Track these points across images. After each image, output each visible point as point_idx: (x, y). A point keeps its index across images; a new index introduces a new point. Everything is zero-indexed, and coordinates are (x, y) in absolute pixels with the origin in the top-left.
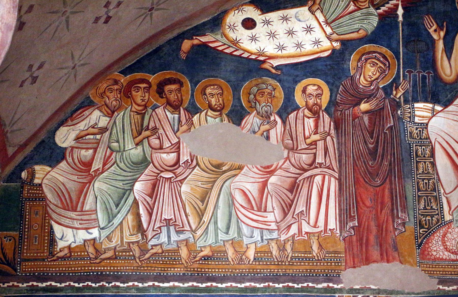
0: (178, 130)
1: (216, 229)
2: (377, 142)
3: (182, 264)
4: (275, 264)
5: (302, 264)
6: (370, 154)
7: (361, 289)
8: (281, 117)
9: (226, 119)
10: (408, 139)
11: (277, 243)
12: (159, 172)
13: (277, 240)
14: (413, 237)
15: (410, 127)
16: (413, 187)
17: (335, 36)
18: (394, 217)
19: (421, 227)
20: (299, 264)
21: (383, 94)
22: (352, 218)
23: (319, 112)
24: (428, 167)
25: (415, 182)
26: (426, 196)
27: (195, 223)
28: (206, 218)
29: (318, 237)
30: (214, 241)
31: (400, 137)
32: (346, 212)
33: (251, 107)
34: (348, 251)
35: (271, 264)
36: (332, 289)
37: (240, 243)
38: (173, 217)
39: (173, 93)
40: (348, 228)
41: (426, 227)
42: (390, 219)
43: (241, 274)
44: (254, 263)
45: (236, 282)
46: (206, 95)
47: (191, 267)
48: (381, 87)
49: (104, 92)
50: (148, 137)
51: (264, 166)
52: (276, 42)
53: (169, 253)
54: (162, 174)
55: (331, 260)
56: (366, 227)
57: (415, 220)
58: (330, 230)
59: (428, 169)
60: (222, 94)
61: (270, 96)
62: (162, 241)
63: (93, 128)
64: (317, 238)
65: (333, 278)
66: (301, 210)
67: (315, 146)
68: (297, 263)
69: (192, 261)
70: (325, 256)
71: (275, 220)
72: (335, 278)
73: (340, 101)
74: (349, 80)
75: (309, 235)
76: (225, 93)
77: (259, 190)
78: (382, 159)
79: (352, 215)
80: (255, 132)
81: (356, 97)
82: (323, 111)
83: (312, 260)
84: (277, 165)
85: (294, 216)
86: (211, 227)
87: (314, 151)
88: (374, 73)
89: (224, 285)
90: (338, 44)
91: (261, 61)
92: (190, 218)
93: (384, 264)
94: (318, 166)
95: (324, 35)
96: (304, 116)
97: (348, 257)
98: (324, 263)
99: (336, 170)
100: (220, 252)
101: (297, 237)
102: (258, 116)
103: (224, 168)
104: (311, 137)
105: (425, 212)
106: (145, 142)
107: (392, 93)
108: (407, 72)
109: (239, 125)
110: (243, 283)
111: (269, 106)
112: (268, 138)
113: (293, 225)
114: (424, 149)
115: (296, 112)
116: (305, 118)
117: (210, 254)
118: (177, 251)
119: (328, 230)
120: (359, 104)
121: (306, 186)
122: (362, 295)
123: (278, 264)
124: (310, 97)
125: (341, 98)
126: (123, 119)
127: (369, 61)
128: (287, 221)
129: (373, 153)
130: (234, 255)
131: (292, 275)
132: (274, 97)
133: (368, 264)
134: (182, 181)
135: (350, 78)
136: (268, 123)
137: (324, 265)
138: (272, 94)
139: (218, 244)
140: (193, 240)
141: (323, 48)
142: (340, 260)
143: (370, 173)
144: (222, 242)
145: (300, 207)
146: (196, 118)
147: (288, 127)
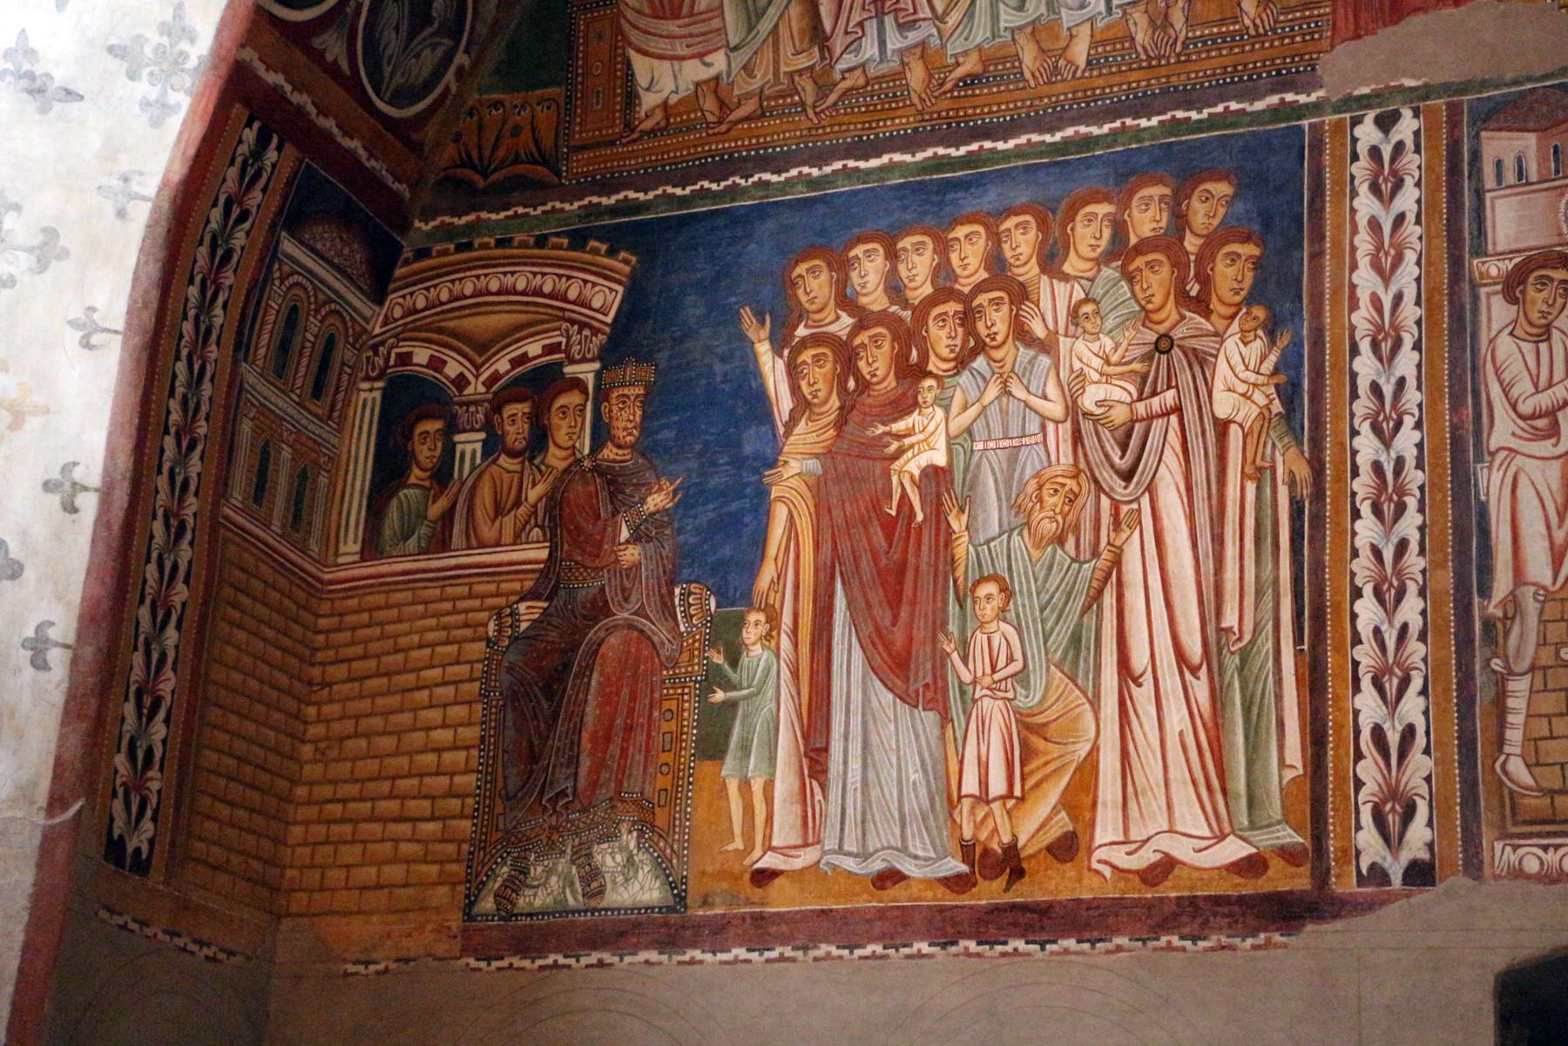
3: (912, 105)
4: (1141, 68)
7: (1377, 94)
11: (1146, 12)
20: (1203, 56)
30: (988, 34)
35: (1131, 70)
37: (1052, 28)
43: (1054, 109)
44: (1087, 74)
45: (1041, 131)
47: (935, 108)
53: (880, 83)
55: (1292, 29)
62: (867, 56)
68: (1199, 53)
69: (936, 94)
70: (1276, 22)
83: (1242, 39)
89: (1011, 144)
93: (1445, 11)
97: (1341, 11)
100: (1004, 59)
110: (1059, 129)
117: (979, 69)
118: (900, 75)
122: (1378, 111)
123: (1150, 67)
130: (1038, 63)
131: (1185, 90)
133: (1397, 22)
137: (1272, 46)
139: (997, 40)
140: (938, 42)
142: (1317, 26)
144: (1008, 35)
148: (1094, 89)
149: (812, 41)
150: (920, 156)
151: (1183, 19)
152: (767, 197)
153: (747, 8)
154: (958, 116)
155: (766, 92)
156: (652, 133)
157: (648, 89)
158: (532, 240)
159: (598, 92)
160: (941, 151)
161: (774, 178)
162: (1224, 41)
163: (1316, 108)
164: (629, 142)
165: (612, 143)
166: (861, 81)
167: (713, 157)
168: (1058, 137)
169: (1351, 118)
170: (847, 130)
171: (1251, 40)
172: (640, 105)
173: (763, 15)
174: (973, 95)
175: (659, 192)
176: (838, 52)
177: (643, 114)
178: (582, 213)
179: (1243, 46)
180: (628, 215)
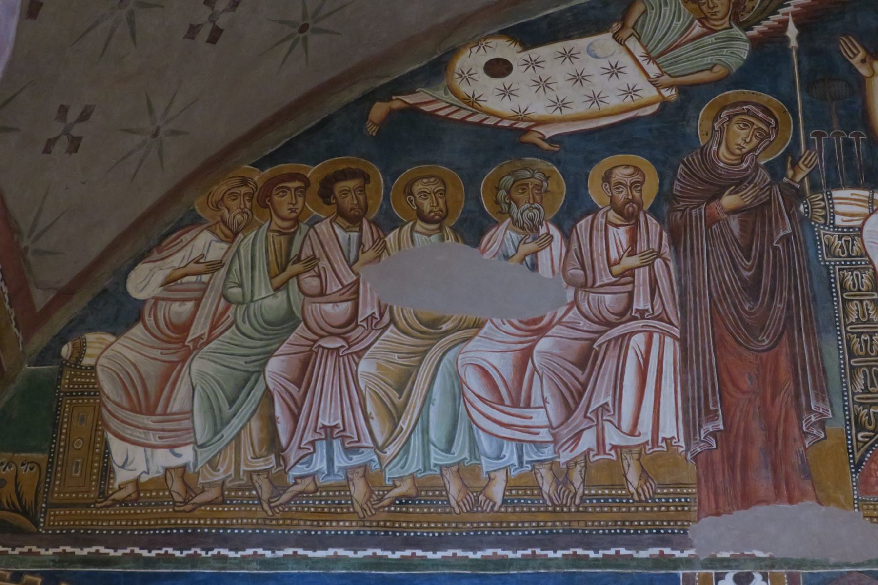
0: (357, 259)
1: (426, 442)
2: (760, 266)
3: (355, 512)
4: (547, 512)
5: (606, 509)
6: (744, 289)
8: (559, 227)
9: (451, 236)
10: (823, 257)
11: (551, 469)
12: (315, 337)
13: (552, 462)
14: (843, 450)
15: (825, 234)
16: (840, 349)
17: (665, 79)
18: (801, 410)
19: (860, 427)
21: (767, 175)
22: (711, 416)
23: (639, 215)
24: (868, 310)
25: (842, 340)
26: (867, 366)
27: (383, 433)
28: (405, 423)
29: (640, 454)
30: (421, 467)
31: (807, 253)
32: (699, 404)
33: (500, 212)
34: (703, 481)
35: (539, 512)
36: (670, 560)
37: (475, 470)
38: (340, 421)
39: (349, 195)
40: (703, 436)
41: (871, 427)
42: (793, 414)
43: (476, 533)
44: (503, 510)
45: (465, 548)
46: (411, 194)
47: (373, 518)
48: (762, 163)
49: (222, 199)
50: (297, 275)
51: (525, 319)
52: (552, 96)
54: (323, 343)
56: (742, 432)
57: (845, 415)
58: (664, 439)
59: (869, 314)
60: (444, 193)
61: (538, 190)
62: (316, 469)
63: (197, 262)
64: (636, 456)
65: (672, 536)
66: (602, 402)
67: (629, 279)
68: (594, 507)
69: (376, 507)
70: (655, 493)
71: (547, 423)
72: (677, 537)
73: (680, 192)
74: (697, 154)
75: (619, 450)
76: (450, 189)
77: (514, 366)
78: (772, 298)
79: (712, 408)
80: (507, 257)
81: (712, 184)
82: (645, 213)
83: (628, 502)
84: (554, 317)
85: (588, 415)
86: (416, 441)
87: (629, 287)
88: (748, 140)
89: (439, 555)
90: (673, 92)
91: (521, 129)
92: (375, 424)
94: (638, 315)
95: (644, 77)
96: (608, 222)
98: (652, 508)
99: (675, 323)
100: (433, 488)
101: (594, 456)
102: (515, 228)
103: (445, 327)
104: (622, 262)
105: (868, 398)
106: (293, 283)
107: (785, 175)
108: (814, 134)
109: (476, 244)
110: (480, 549)
111: (536, 208)
112: (534, 267)
113: (585, 433)
114: (857, 276)
115: (590, 218)
116: (610, 228)
117: (413, 492)
118: (345, 487)
119: (660, 440)
120: (718, 196)
121: (613, 354)
122: (736, 572)
123: (554, 512)
124: (618, 188)
125: (682, 187)
126: (253, 244)
127: (736, 118)
128: (574, 424)
129: (752, 288)
130: (462, 495)
132: (546, 191)
134: (360, 354)
135: (699, 150)
136: (534, 239)
138: (542, 186)
139: (428, 473)
140: (378, 466)
141: (643, 101)
142: (686, 501)
143: (746, 326)
144: (437, 469)
145: (602, 397)
146: (391, 238)
147: (575, 245)
148: (509, 522)
149: (270, 451)
150: (361, 554)
151: (581, 480)
152: (224, 569)
153: (214, 417)
154: (393, 527)
155: (228, 484)
156: (124, 502)
157: (123, 467)
158: (8, 575)
159: (77, 463)
160: (379, 552)
161: (232, 554)
162: (614, 501)
163: (688, 563)
164: (102, 507)
165: (88, 506)
166: (311, 488)
167: (178, 530)
168: (479, 555)
169: (716, 574)
170: (298, 525)
171: (636, 504)
172: (114, 478)
173: (228, 422)
174: (407, 512)
175: (128, 551)
176: (292, 461)
177: (116, 486)
178: (57, 558)
179: (629, 507)
180: (98, 566)
